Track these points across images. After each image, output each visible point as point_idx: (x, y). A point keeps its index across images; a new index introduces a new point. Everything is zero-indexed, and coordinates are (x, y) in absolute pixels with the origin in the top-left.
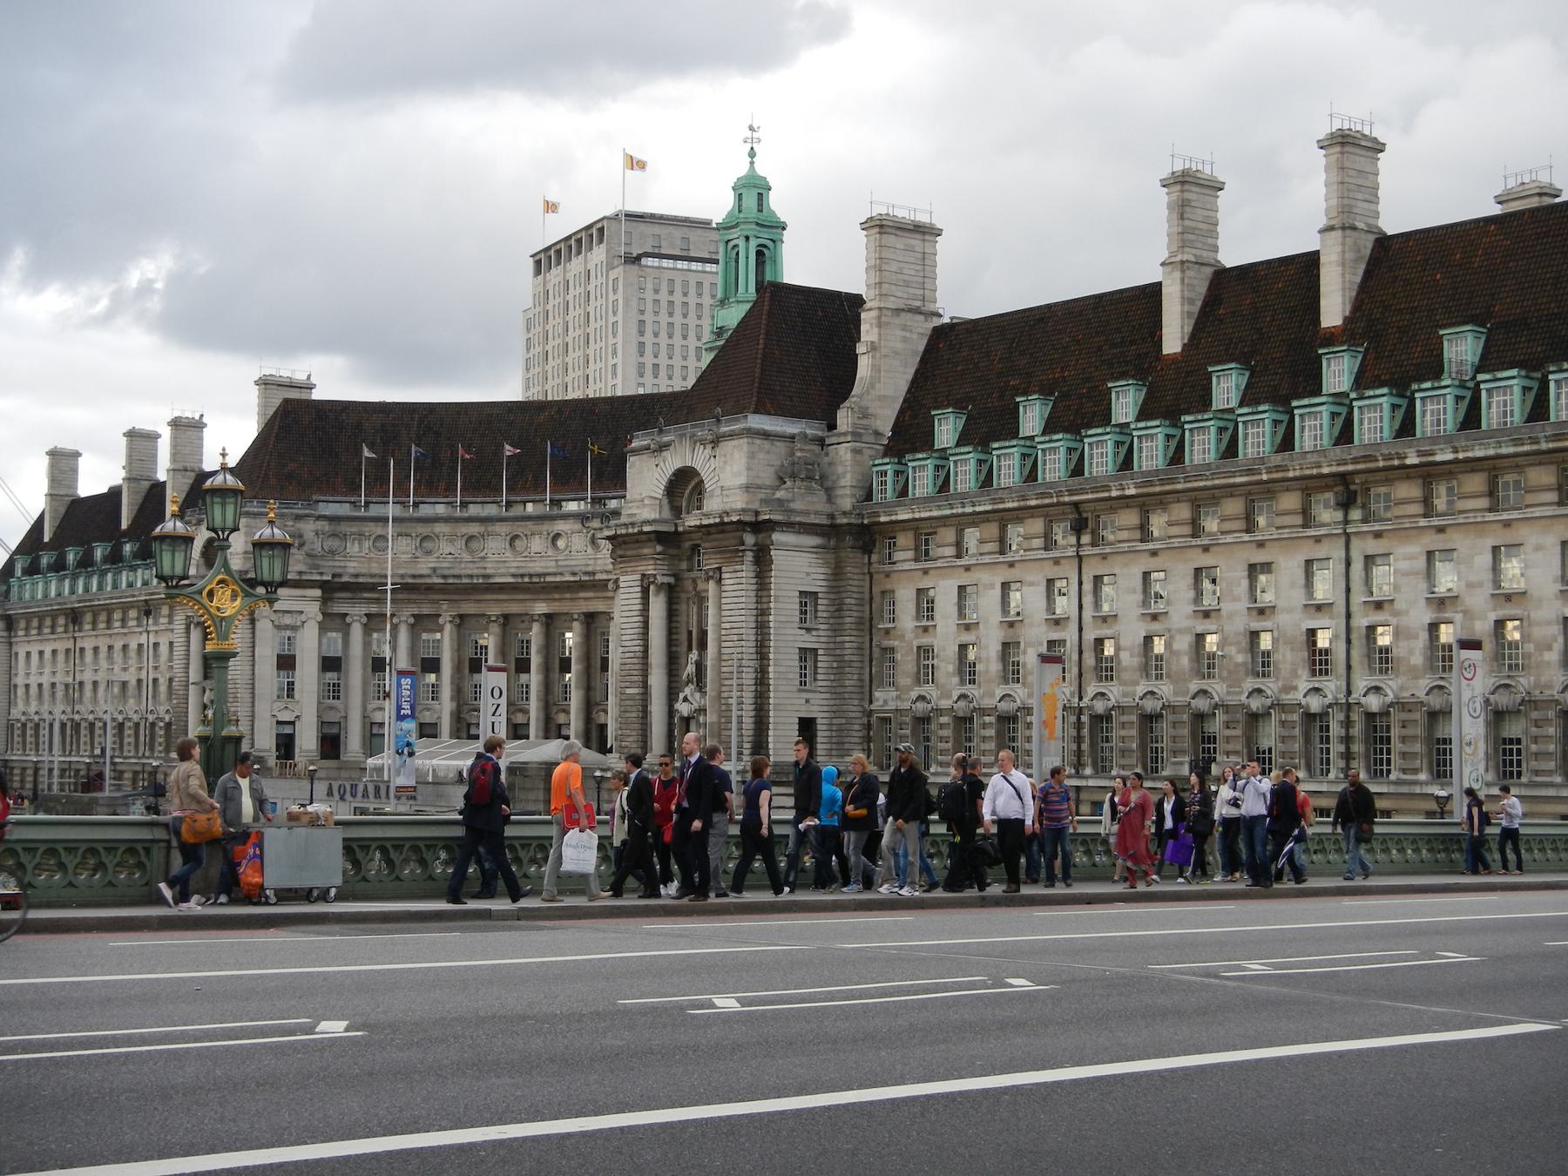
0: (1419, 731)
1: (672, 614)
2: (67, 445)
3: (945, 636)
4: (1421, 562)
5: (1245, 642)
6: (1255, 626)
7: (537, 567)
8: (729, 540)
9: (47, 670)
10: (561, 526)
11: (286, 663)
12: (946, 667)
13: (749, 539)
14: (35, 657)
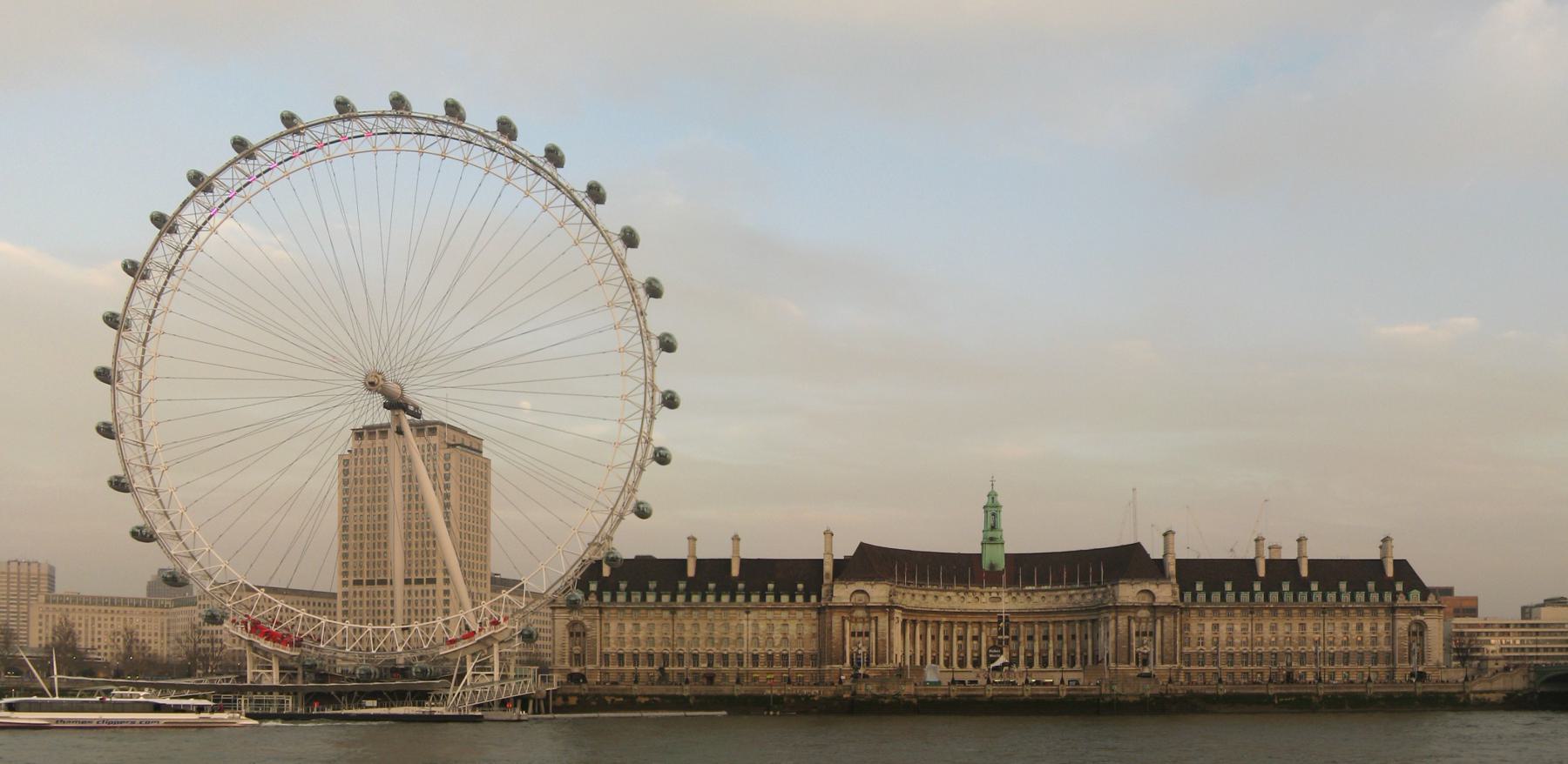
14: (629, 626)
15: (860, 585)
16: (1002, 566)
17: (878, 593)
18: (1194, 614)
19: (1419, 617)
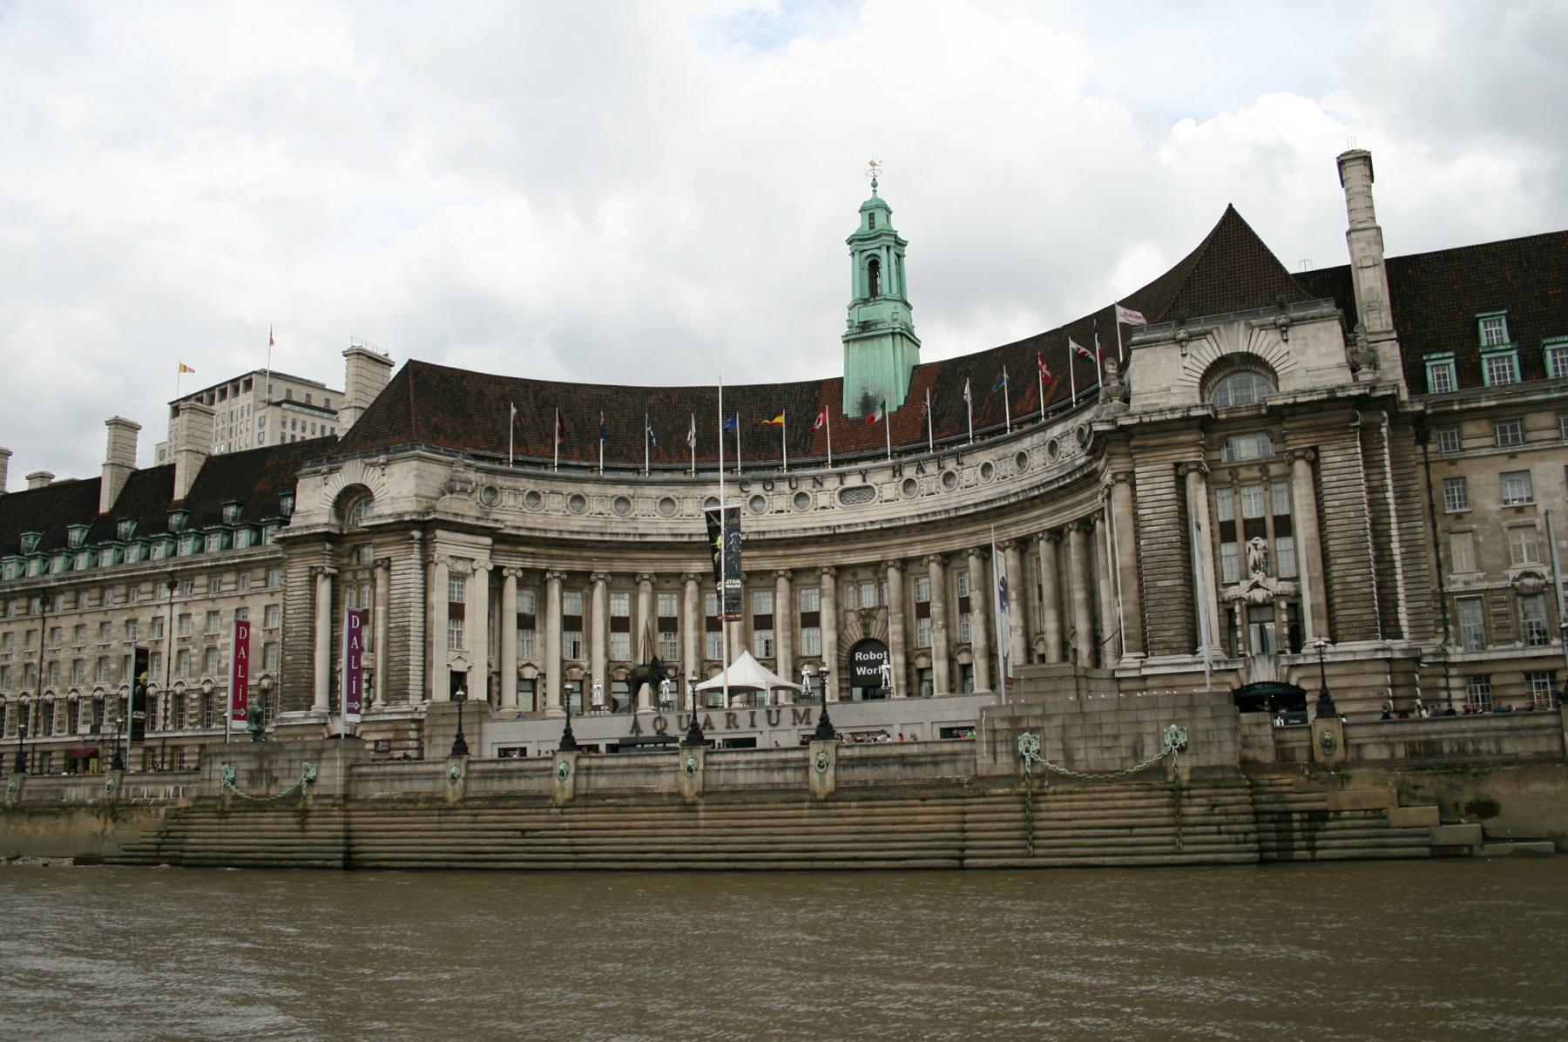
8: (1338, 417)
11: (457, 612)
15: (351, 473)
16: (896, 397)
17: (398, 486)
18: (1476, 437)
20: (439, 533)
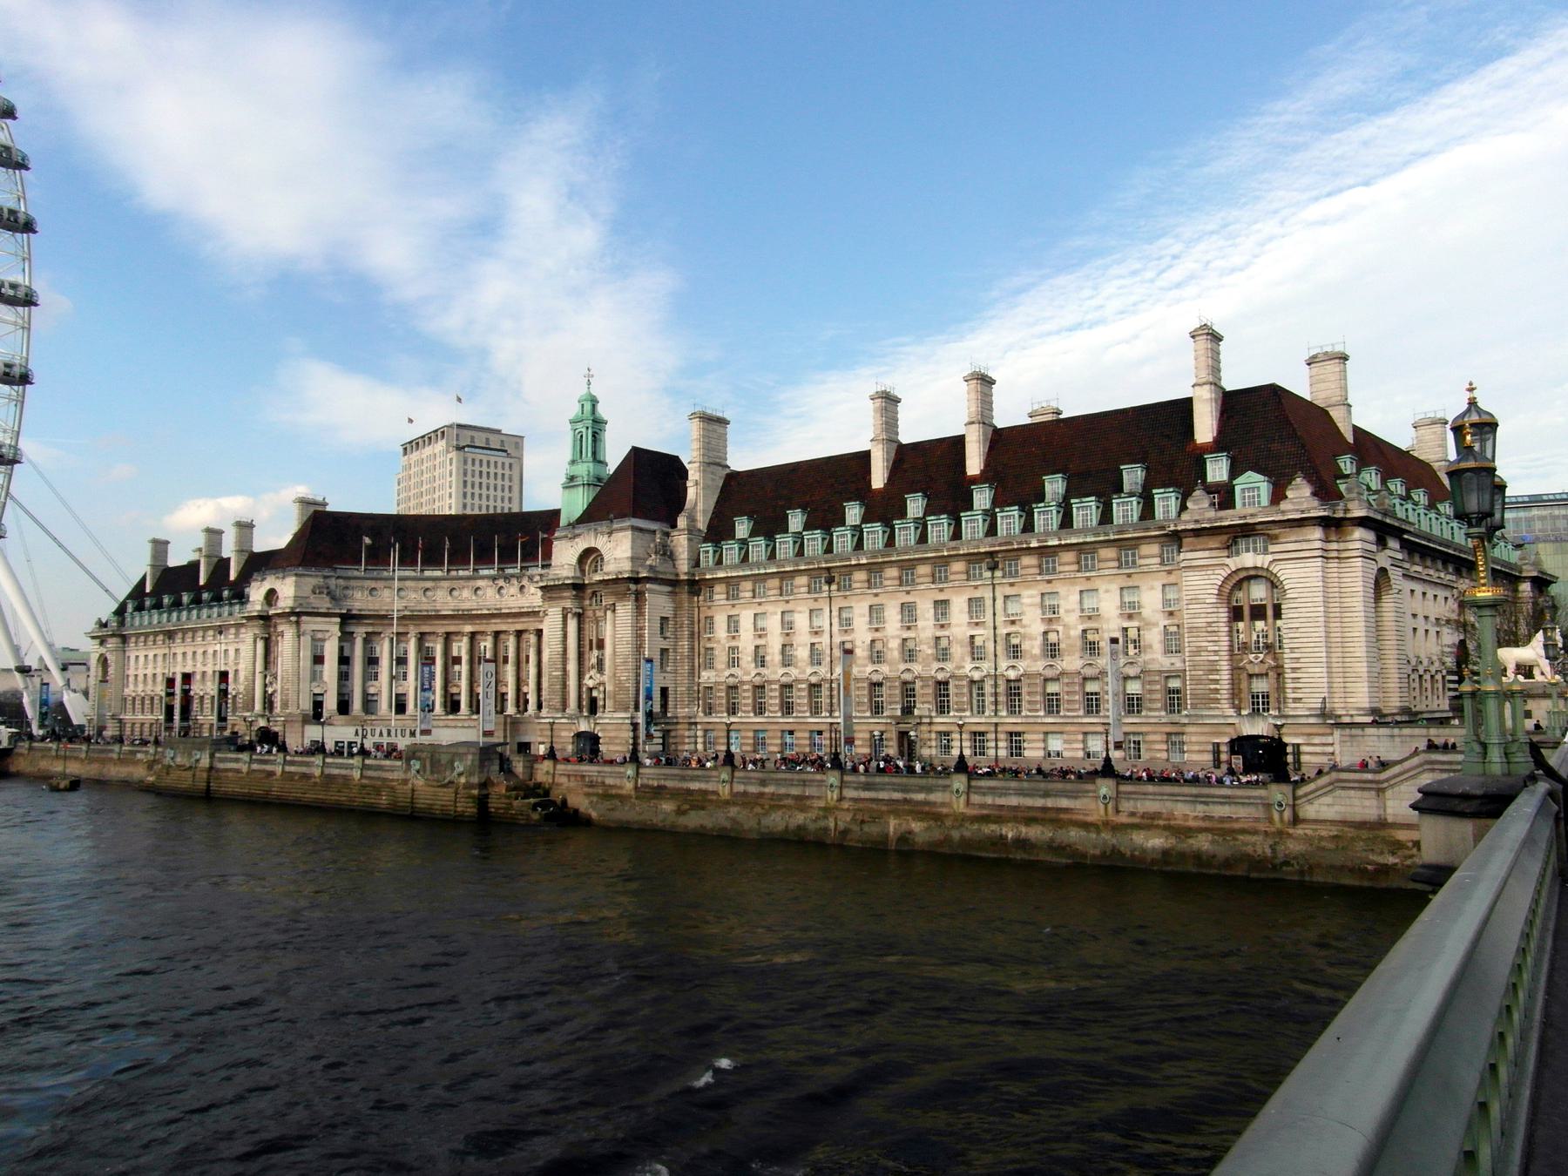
0: (1039, 689)
1: (580, 630)
2: (161, 536)
3: (747, 641)
4: (1038, 599)
5: (932, 643)
6: (939, 634)
7: (466, 605)
8: (621, 587)
9: (150, 666)
10: (480, 583)
12: (747, 658)
13: (633, 587)
14: (142, 659)
17: (287, 589)
19: (1249, 559)
20: (304, 618)
